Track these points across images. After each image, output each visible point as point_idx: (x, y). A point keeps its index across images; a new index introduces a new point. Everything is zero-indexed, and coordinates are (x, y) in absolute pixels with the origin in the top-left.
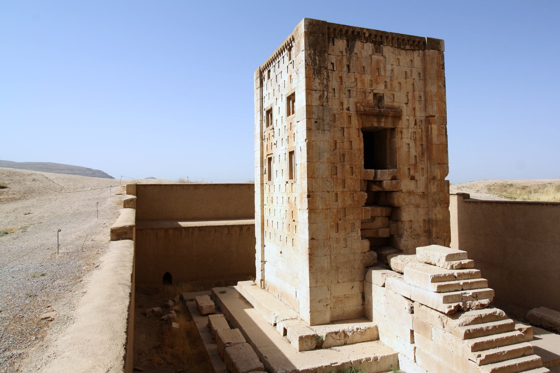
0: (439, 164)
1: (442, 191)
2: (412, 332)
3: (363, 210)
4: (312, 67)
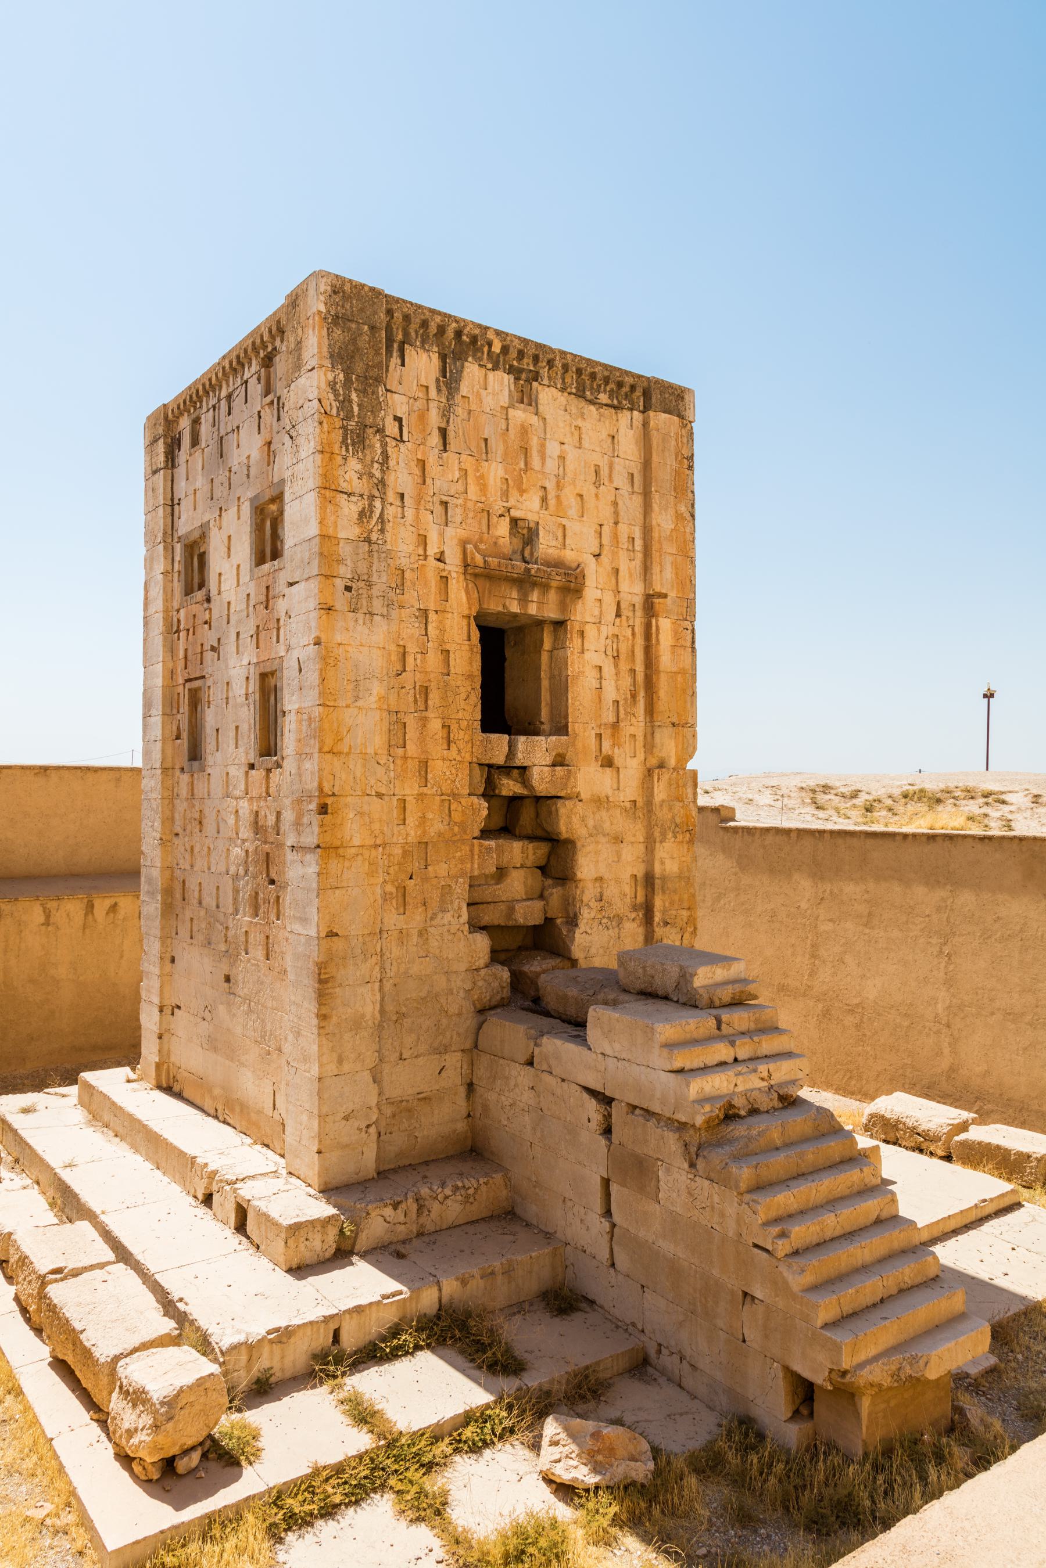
0: (674, 725)
1: (680, 799)
2: (606, 1183)
3: (476, 849)
4: (338, 423)
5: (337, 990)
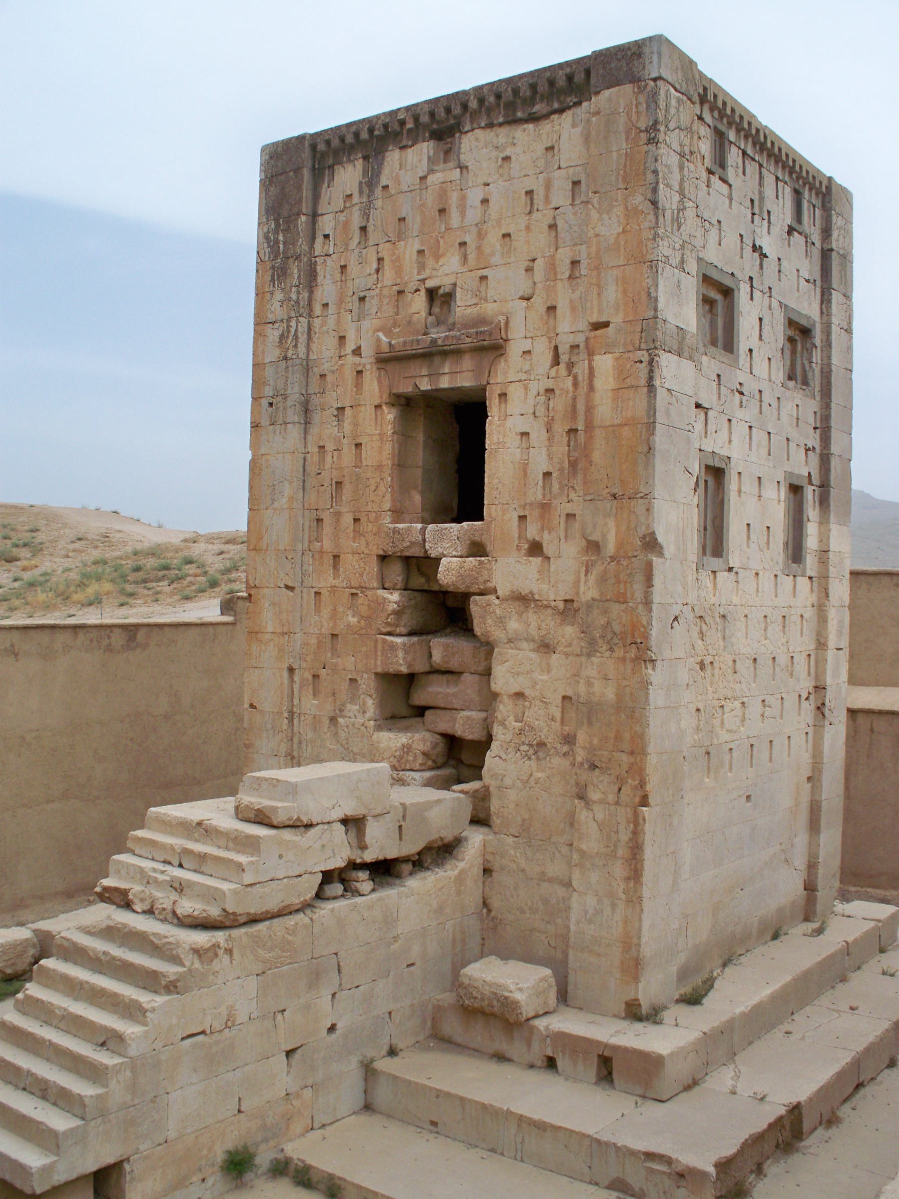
0: (614, 496)
1: (622, 599)
3: (380, 645)
4: (269, 265)
5: (255, 756)
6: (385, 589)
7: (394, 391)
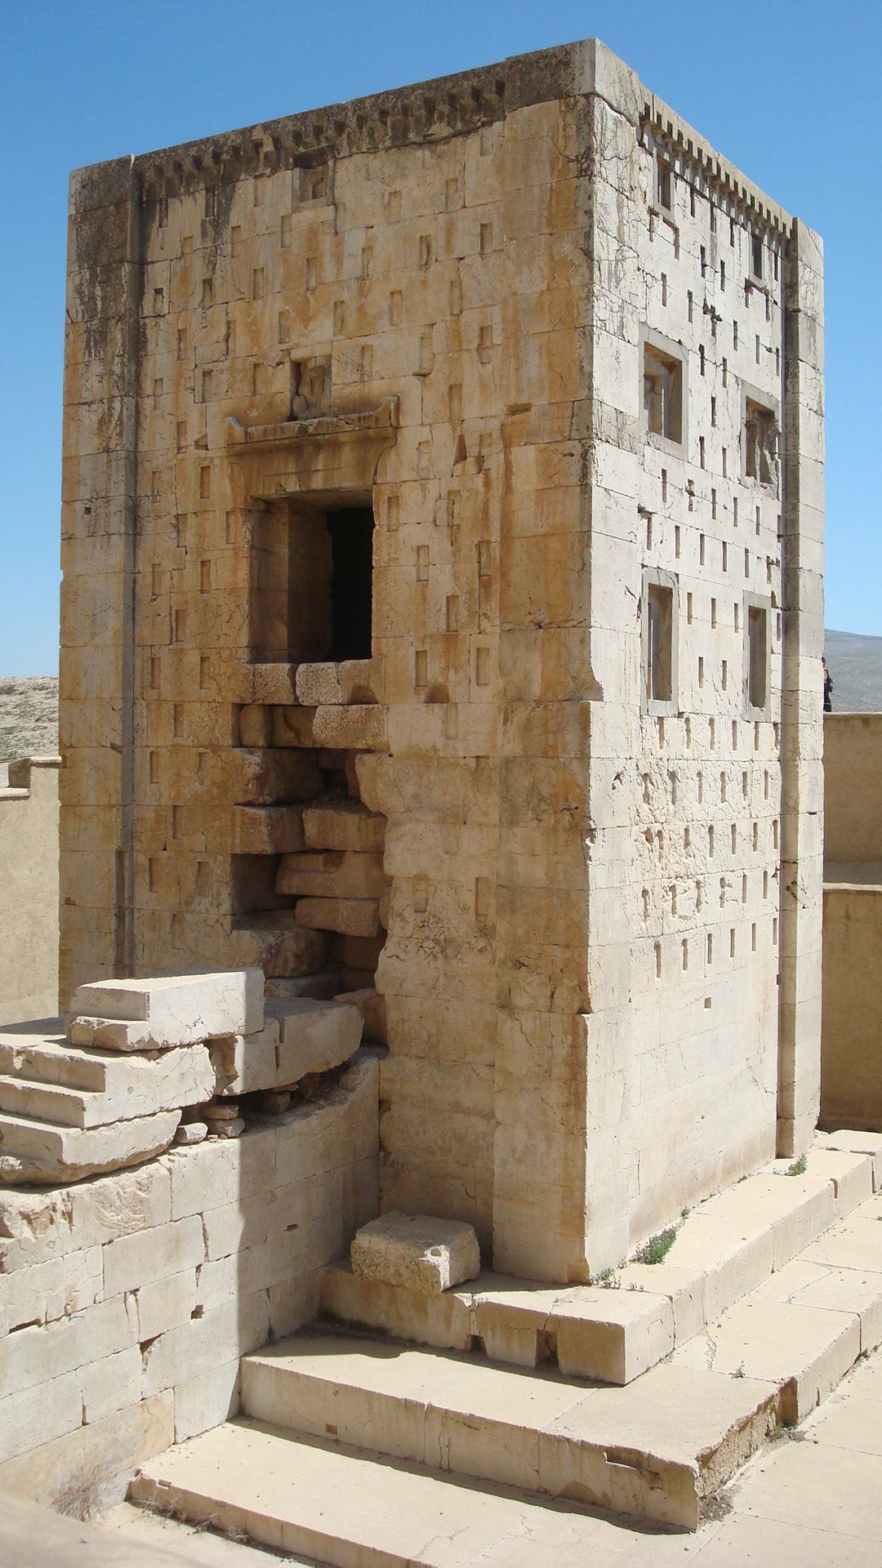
4: (83, 327)
6: (241, 745)
7: (253, 493)
